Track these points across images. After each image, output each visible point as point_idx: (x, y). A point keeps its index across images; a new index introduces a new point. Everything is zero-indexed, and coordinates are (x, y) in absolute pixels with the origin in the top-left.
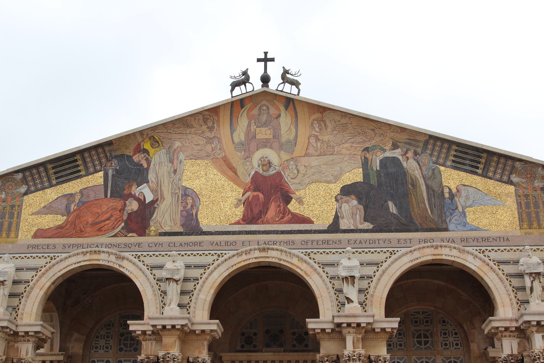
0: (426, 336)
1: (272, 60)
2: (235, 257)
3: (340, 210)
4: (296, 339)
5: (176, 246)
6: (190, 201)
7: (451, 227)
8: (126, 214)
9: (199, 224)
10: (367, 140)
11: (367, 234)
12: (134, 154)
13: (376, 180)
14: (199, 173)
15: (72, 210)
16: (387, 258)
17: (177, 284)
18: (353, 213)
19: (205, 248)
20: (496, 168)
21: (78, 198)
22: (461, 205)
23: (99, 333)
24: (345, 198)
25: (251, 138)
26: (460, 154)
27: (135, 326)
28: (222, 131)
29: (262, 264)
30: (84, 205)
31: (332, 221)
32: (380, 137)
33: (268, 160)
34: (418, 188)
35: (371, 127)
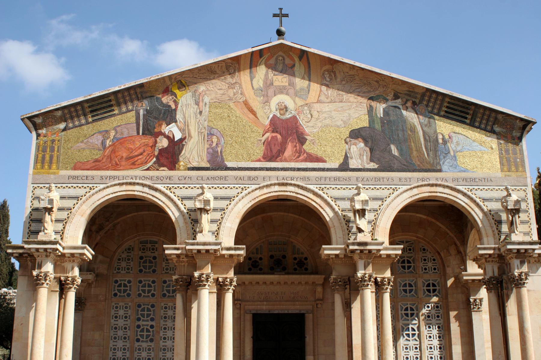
0: (409, 262)
1: (287, 16)
2: (258, 191)
3: (349, 151)
4: (297, 264)
5: (203, 179)
6: (215, 140)
7: (444, 168)
8: (158, 150)
9: (223, 161)
10: (372, 90)
11: (373, 173)
12: (163, 97)
13: (380, 126)
14: (222, 115)
15: (108, 145)
16: (390, 194)
17: (208, 214)
18: (360, 154)
19: (230, 182)
20: (482, 119)
21: (112, 133)
22: (453, 150)
23: (120, 256)
24: (353, 141)
25: (269, 85)
26: (452, 106)
27: (170, 251)
28: (242, 78)
29: (280, 198)
30: (119, 142)
31: (342, 161)
32: (383, 88)
33: (285, 105)
34: (416, 133)
35: (376, 79)
